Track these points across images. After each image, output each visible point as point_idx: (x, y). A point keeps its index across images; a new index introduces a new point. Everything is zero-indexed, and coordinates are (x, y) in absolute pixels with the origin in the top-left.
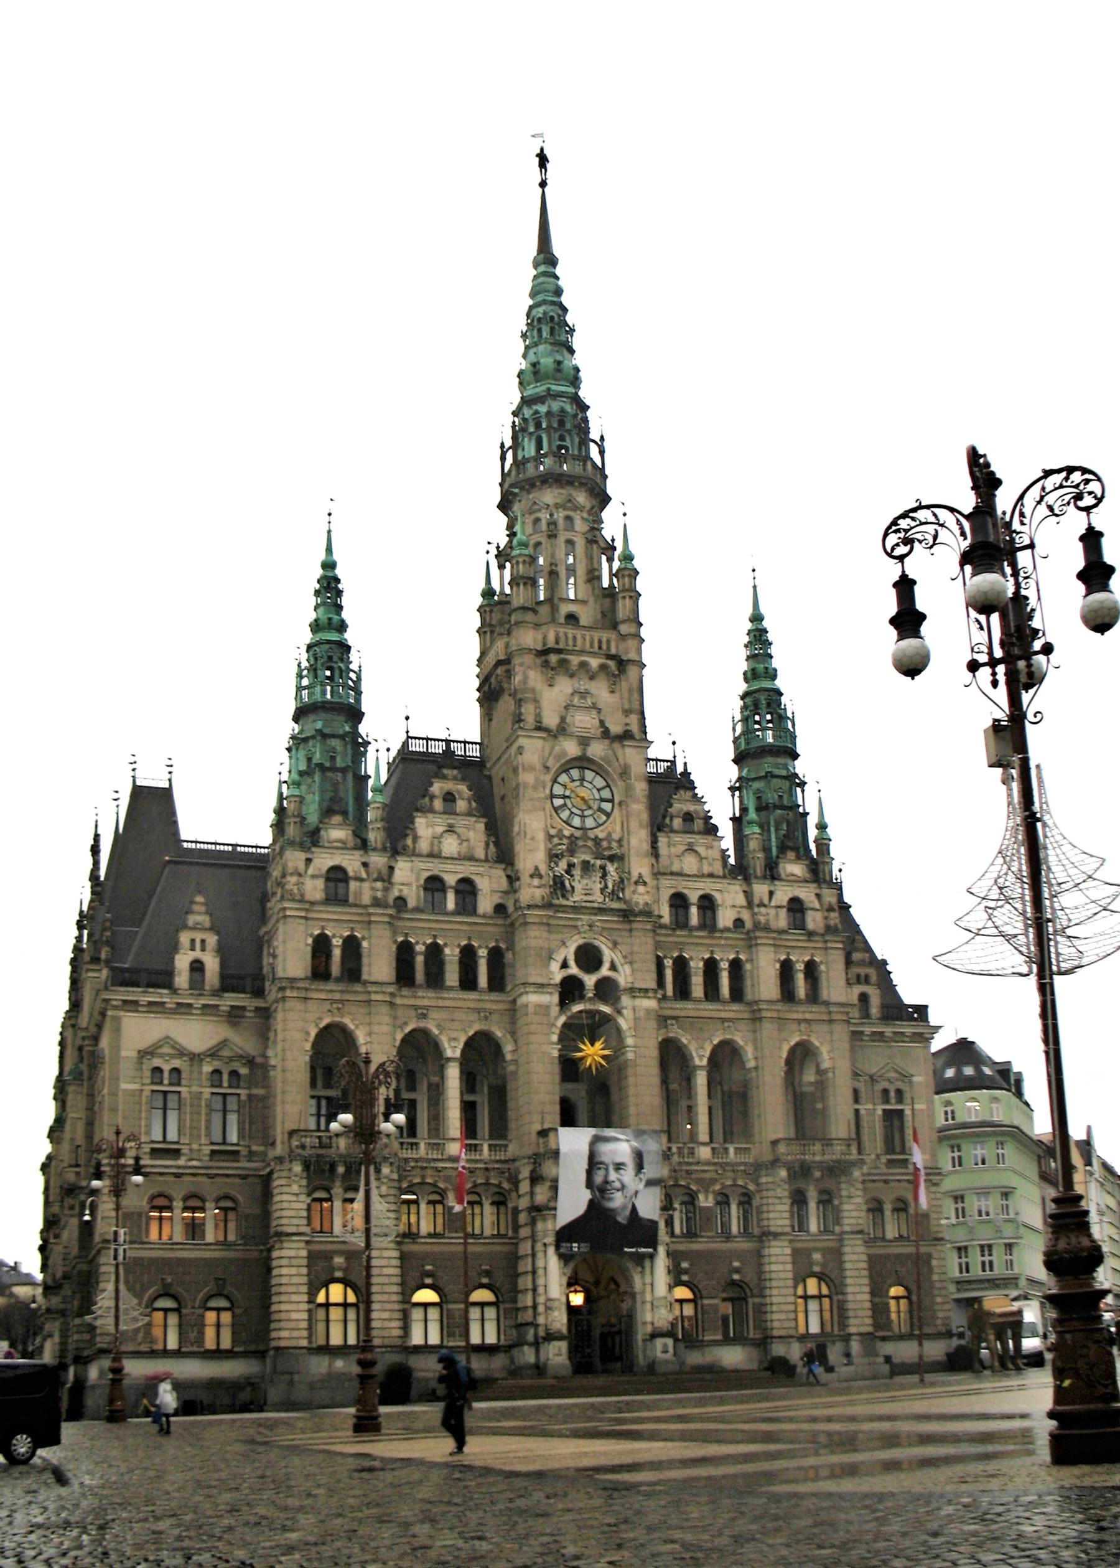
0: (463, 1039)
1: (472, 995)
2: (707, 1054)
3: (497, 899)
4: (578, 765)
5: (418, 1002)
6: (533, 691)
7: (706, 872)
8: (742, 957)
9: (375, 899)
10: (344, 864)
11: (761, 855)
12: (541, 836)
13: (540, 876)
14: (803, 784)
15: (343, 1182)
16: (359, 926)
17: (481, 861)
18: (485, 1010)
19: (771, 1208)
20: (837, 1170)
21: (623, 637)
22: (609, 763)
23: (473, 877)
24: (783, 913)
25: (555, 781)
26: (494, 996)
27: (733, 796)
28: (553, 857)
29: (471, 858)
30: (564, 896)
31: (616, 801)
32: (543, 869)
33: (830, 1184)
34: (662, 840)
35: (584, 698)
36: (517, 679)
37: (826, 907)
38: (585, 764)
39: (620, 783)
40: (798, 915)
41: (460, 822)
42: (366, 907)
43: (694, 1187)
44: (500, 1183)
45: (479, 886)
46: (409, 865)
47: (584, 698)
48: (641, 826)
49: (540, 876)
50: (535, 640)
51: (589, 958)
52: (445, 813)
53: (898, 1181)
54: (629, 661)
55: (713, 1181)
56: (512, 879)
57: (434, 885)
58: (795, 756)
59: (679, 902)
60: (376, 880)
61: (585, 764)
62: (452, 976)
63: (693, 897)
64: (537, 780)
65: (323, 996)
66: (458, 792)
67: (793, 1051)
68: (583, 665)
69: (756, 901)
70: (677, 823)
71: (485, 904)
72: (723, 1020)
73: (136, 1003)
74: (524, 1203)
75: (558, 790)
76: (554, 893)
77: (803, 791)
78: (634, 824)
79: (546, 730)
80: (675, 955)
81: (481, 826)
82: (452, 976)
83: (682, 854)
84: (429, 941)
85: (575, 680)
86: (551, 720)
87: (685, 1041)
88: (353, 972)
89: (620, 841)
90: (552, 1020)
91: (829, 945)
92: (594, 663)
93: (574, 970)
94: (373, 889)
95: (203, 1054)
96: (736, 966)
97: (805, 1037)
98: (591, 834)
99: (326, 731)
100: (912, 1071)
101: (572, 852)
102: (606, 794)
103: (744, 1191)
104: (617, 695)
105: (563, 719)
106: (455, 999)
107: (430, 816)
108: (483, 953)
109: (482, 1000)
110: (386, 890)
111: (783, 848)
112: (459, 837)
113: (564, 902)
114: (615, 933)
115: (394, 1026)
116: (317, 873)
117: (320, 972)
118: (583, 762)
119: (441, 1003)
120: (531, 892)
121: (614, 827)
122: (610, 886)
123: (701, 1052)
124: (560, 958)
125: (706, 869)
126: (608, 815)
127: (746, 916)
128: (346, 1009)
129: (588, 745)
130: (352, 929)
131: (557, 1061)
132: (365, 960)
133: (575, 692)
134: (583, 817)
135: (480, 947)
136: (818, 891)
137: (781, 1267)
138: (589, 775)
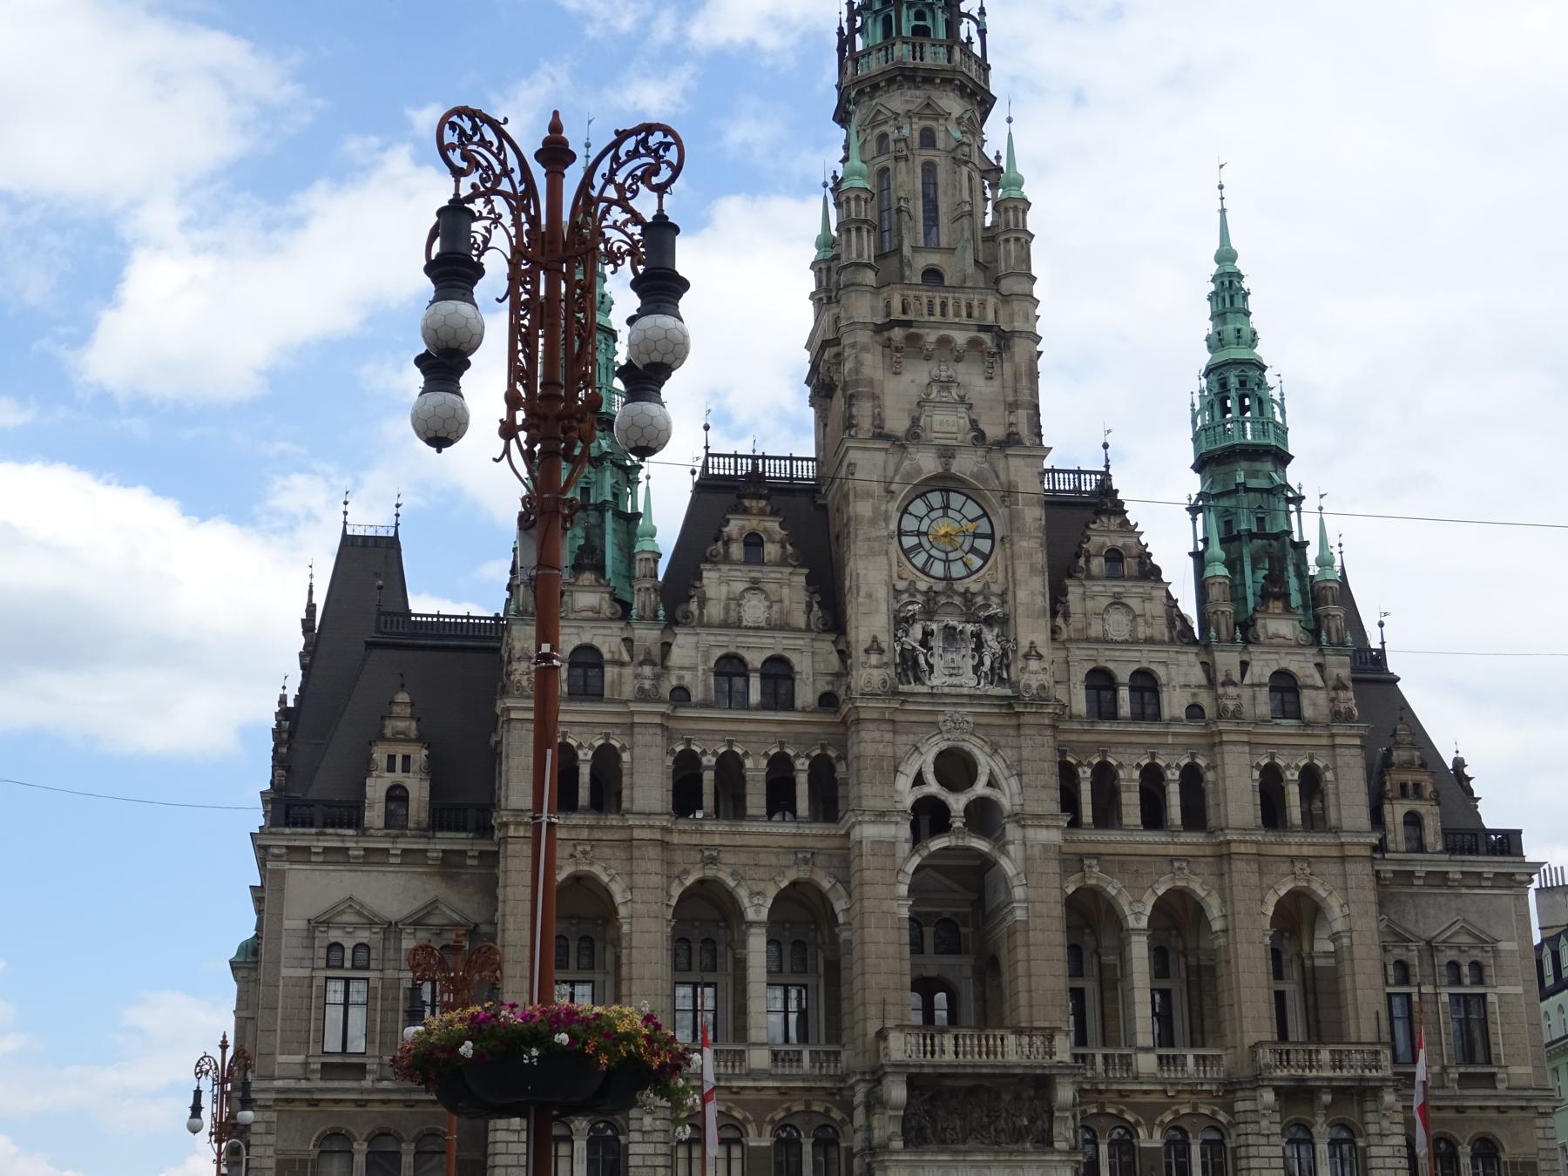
0: (772, 892)
3: (823, 686)
4: (941, 484)
5: (706, 840)
6: (871, 382)
7: (1141, 636)
8: (1201, 762)
9: (641, 690)
10: (597, 642)
11: (1228, 608)
12: (882, 593)
13: (881, 651)
14: (1299, 499)
16: (617, 731)
17: (800, 630)
18: (804, 849)
19: (1253, 1151)
20: (1362, 1093)
21: (1006, 299)
22: (985, 481)
23: (787, 654)
24: (1264, 694)
25: (905, 511)
26: (818, 828)
27: (1194, 520)
28: (901, 622)
30: (918, 680)
31: (998, 536)
32: (885, 639)
33: (1351, 1116)
34: (1074, 591)
35: (948, 388)
36: (848, 366)
37: (1331, 683)
38: (949, 484)
39: (1002, 511)
40: (1289, 697)
41: (770, 576)
42: (625, 702)
43: (1129, 1117)
44: (828, 1110)
45: (797, 668)
46: (693, 639)
47: (948, 388)
48: (1033, 570)
49: (881, 651)
50: (873, 308)
51: (956, 769)
52: (746, 562)
53: (1481, 1108)
54: (1013, 332)
55: (1162, 1108)
56: (844, 655)
57: (730, 667)
58: (1283, 458)
59: (1100, 681)
60: (641, 664)
62: (756, 800)
63: (1123, 674)
64: (875, 509)
66: (766, 530)
68: (944, 342)
69: (1221, 678)
70: (1097, 564)
71: (806, 694)
72: (1172, 859)
74: (858, 1142)
75: (909, 524)
76: (902, 677)
77: (1299, 511)
78: (1022, 570)
80: (1095, 761)
81: (800, 580)
82: (756, 800)
83: (1106, 610)
84: (722, 750)
85: (931, 364)
86: (897, 423)
89: (1002, 596)
90: (899, 862)
91: (1338, 741)
92: (960, 338)
93: (933, 787)
96: (1192, 778)
100: (1496, 932)
101: (929, 613)
102: (984, 526)
104: (997, 382)
105: (915, 421)
107: (725, 568)
108: (802, 764)
111: (1265, 596)
112: (767, 598)
114: (996, 732)
115: (669, 877)
118: (946, 483)
120: (869, 674)
121: (994, 575)
122: (987, 661)
124: (910, 770)
125: (1143, 631)
126: (986, 558)
127: (1205, 699)
129: (953, 456)
130: (607, 736)
131: (907, 924)
132: (625, 780)
133: (935, 381)
134: (947, 561)
135: (797, 756)
136: (1319, 660)
138: (956, 500)
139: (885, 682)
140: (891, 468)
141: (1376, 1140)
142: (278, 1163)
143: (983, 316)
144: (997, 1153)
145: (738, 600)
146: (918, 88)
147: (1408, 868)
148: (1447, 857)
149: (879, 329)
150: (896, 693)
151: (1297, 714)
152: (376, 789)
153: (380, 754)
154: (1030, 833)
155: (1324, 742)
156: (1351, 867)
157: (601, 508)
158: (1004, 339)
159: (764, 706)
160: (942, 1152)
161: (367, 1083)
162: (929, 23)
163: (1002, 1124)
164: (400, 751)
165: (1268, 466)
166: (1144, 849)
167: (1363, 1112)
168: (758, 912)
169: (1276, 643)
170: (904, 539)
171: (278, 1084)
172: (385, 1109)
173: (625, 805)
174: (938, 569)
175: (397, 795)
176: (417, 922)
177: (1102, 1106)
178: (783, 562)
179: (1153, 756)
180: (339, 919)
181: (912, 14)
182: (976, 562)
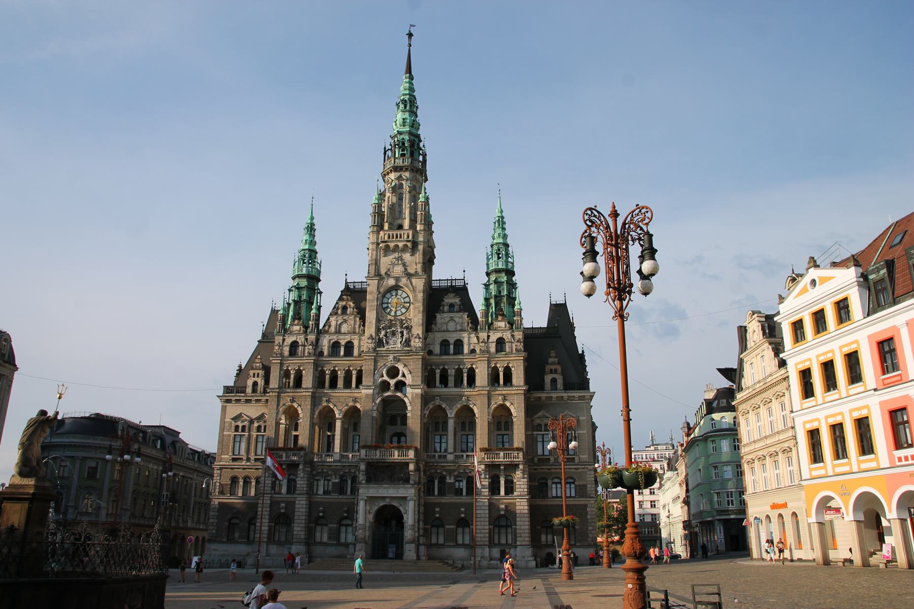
1: (348, 391)
2: (455, 412)
4: (395, 288)
7: (458, 329)
12: (374, 321)
28: (378, 330)
34: (438, 316)
37: (516, 340)
43: (444, 473)
51: (393, 372)
55: (455, 470)
57: (335, 346)
59: (445, 344)
60: (310, 345)
63: (452, 341)
68: (397, 246)
69: (481, 341)
70: (446, 308)
71: (356, 352)
82: (340, 383)
87: (444, 406)
92: (401, 245)
95: (254, 419)
98: (399, 318)
102: (407, 300)
108: (354, 372)
123: (451, 411)
125: (459, 328)
126: (407, 309)
137: (482, 512)
144: (391, 484)
148: (564, 391)
152: (250, 382)
160: (374, 484)
162: (405, 152)
164: (256, 372)
173: (303, 386)
174: (393, 314)
175: (255, 384)
177: (436, 470)
182: (404, 310)
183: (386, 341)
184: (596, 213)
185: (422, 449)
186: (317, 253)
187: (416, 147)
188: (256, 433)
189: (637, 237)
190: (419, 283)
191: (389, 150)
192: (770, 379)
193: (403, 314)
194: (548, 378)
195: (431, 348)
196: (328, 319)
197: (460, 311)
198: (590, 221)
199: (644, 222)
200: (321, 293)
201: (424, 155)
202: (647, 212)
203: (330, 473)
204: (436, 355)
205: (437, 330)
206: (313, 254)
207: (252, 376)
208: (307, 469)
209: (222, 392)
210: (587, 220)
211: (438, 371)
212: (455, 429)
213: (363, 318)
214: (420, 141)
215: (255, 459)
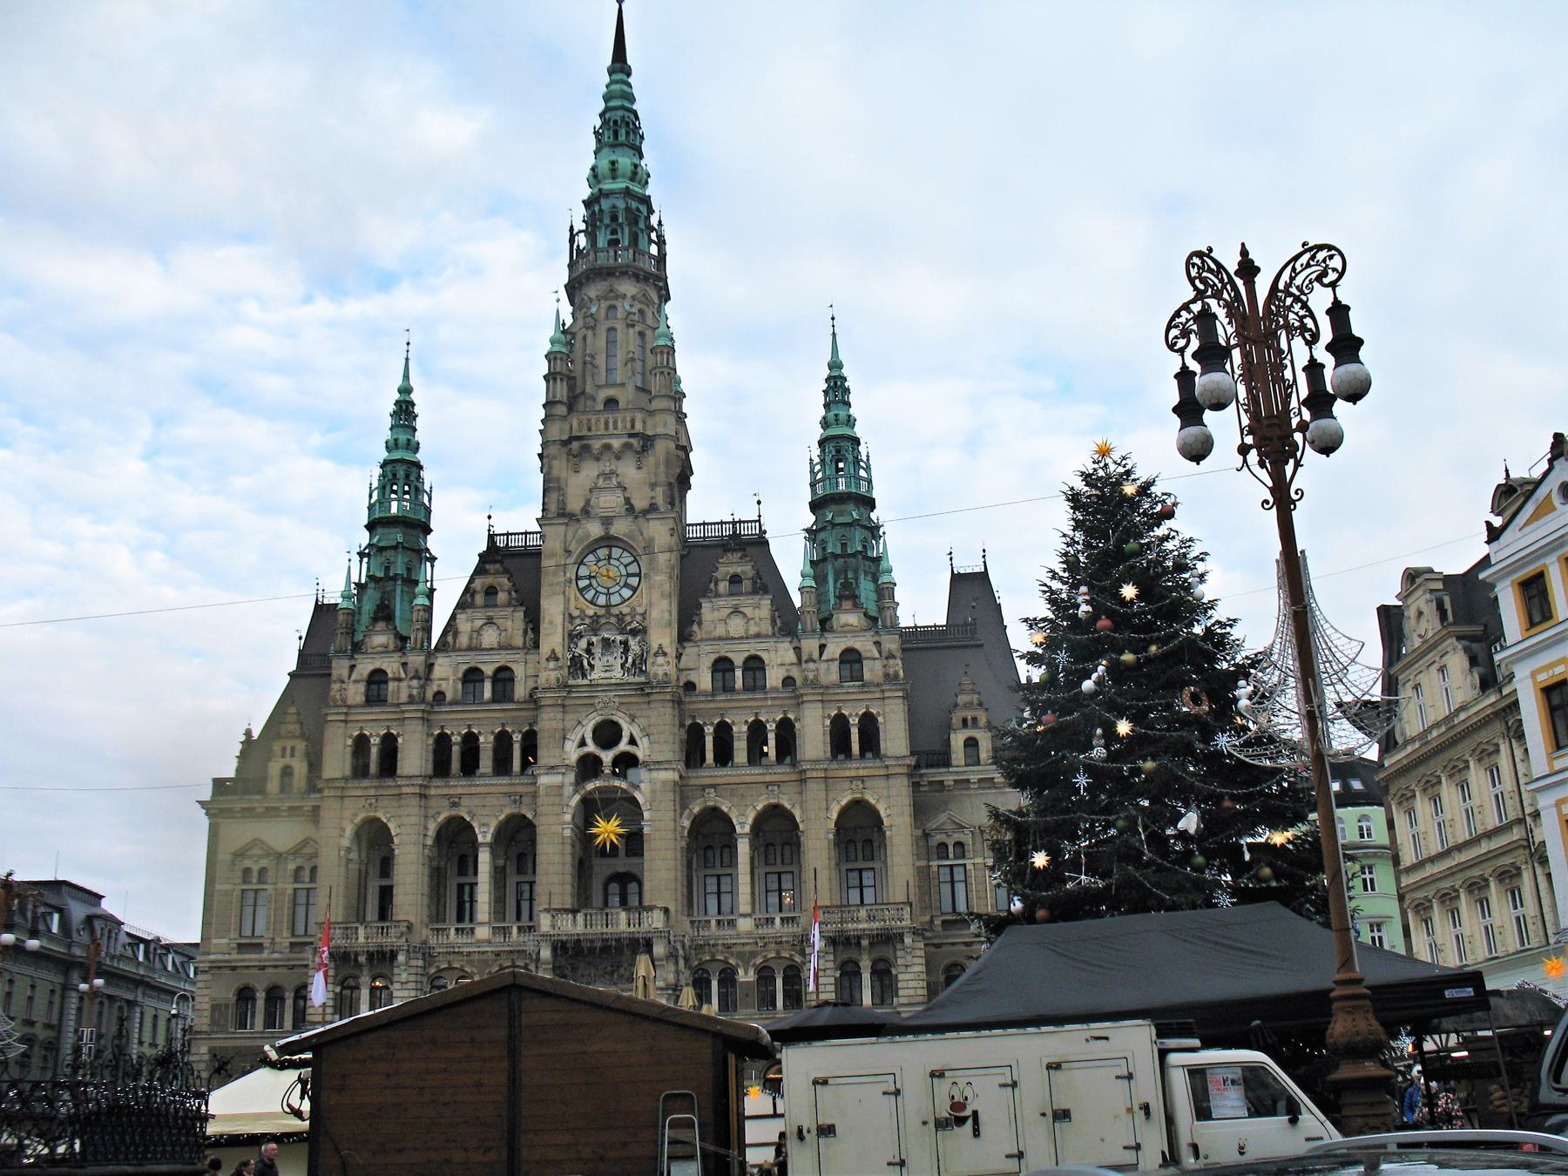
1: (505, 780)
2: (750, 820)
3: (531, 684)
5: (452, 791)
6: (558, 480)
8: (791, 716)
9: (410, 696)
12: (559, 619)
13: (557, 659)
15: (370, 970)
16: (395, 724)
17: (519, 648)
18: (515, 794)
20: (888, 939)
23: (509, 665)
24: (835, 666)
28: (573, 637)
29: (511, 648)
30: (584, 676)
34: (706, 606)
35: (610, 479)
37: (884, 654)
42: (398, 705)
47: (610, 479)
49: (557, 659)
51: (607, 734)
52: (486, 606)
55: (754, 954)
57: (472, 676)
59: (722, 666)
60: (412, 679)
61: (615, 543)
62: (486, 763)
63: (738, 660)
65: (359, 793)
66: (499, 584)
67: (844, 812)
68: (607, 447)
69: (804, 657)
70: (723, 586)
71: (520, 691)
72: (768, 784)
73: (231, 810)
79: (571, 516)
81: (520, 615)
82: (486, 763)
85: (601, 463)
86: (575, 505)
88: (389, 763)
89: (643, 615)
90: (565, 798)
91: (887, 694)
92: (616, 444)
93: (591, 747)
94: (410, 687)
95: (288, 853)
97: (859, 796)
98: (615, 611)
99: (382, 544)
101: (595, 627)
102: (633, 569)
103: (791, 963)
105: (588, 502)
106: (486, 785)
107: (469, 611)
108: (517, 737)
109: (514, 784)
110: (423, 687)
111: (840, 597)
113: (580, 681)
114: (632, 707)
116: (359, 678)
117: (360, 771)
118: (608, 541)
119: (473, 790)
121: (640, 603)
122: (630, 660)
124: (575, 737)
125: (753, 630)
126: (635, 590)
127: (795, 673)
128: (380, 803)
130: (388, 727)
133: (602, 474)
134: (608, 594)
136: (877, 639)
138: (616, 552)
139: (558, 680)
140: (570, 535)
141: (902, 969)
142: (213, 1006)
143: (633, 426)
145: (479, 631)
146: (605, 280)
147: (965, 777)
149: (565, 443)
150: (566, 686)
151: (863, 680)
152: (275, 769)
153: (277, 747)
154: (654, 774)
155: (877, 696)
156: (892, 781)
157: (394, 578)
158: (647, 442)
159: (494, 700)
161: (265, 955)
163: (622, 971)
164: (289, 744)
165: (850, 507)
166: (748, 779)
167: (895, 949)
168: (484, 837)
169: (847, 630)
170: (579, 582)
171: (212, 957)
172: (276, 971)
173: (399, 771)
175: (287, 772)
176: (296, 852)
178: (509, 604)
179: (756, 714)
180: (250, 853)
181: (608, 232)
182: (626, 593)
183: (589, 664)
184: (1213, 266)
185: (680, 909)
186: (421, 468)
187: (642, 225)
188: (291, 886)
189: (1297, 324)
190: (659, 532)
191: (580, 231)
192: (1462, 716)
193: (625, 601)
194: (958, 740)
195: (693, 677)
196: (453, 617)
197: (755, 592)
198: (1204, 281)
199: (1326, 281)
200: (433, 559)
201: (661, 242)
202: (1331, 257)
203: (468, 969)
204: (705, 694)
205: (704, 636)
206: (414, 470)
207: (279, 753)
208: (414, 962)
209: (210, 794)
210: (1195, 278)
211: (709, 730)
212: (752, 859)
213: (533, 621)
214: (651, 211)
215: (291, 943)
